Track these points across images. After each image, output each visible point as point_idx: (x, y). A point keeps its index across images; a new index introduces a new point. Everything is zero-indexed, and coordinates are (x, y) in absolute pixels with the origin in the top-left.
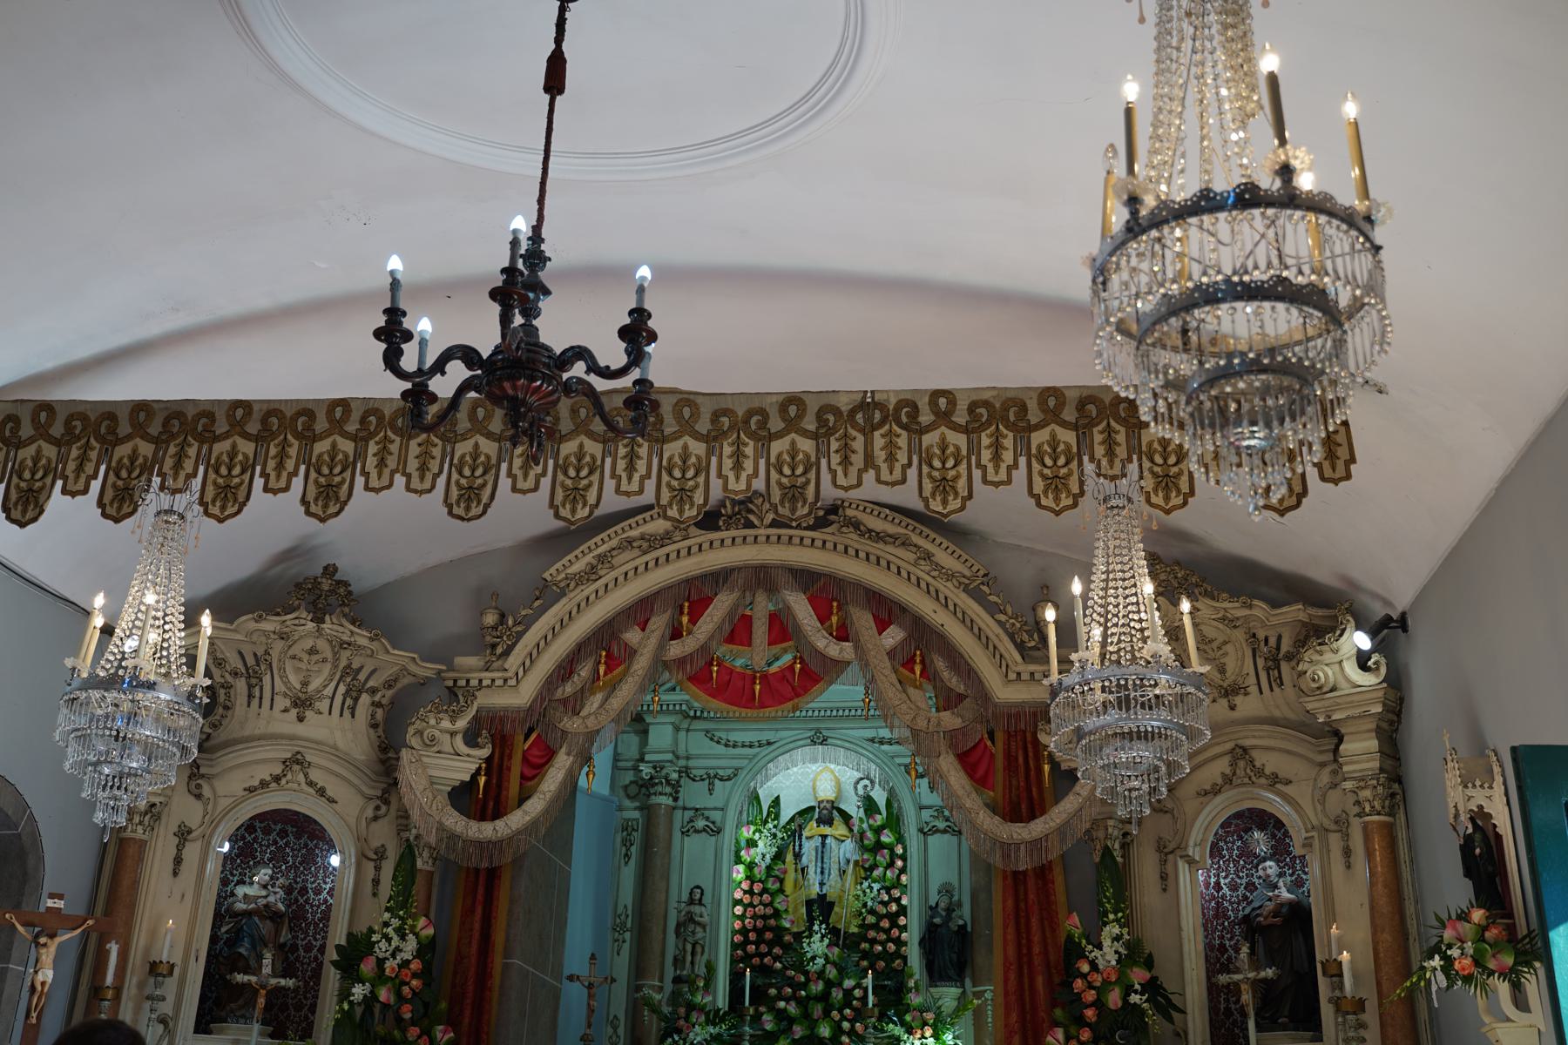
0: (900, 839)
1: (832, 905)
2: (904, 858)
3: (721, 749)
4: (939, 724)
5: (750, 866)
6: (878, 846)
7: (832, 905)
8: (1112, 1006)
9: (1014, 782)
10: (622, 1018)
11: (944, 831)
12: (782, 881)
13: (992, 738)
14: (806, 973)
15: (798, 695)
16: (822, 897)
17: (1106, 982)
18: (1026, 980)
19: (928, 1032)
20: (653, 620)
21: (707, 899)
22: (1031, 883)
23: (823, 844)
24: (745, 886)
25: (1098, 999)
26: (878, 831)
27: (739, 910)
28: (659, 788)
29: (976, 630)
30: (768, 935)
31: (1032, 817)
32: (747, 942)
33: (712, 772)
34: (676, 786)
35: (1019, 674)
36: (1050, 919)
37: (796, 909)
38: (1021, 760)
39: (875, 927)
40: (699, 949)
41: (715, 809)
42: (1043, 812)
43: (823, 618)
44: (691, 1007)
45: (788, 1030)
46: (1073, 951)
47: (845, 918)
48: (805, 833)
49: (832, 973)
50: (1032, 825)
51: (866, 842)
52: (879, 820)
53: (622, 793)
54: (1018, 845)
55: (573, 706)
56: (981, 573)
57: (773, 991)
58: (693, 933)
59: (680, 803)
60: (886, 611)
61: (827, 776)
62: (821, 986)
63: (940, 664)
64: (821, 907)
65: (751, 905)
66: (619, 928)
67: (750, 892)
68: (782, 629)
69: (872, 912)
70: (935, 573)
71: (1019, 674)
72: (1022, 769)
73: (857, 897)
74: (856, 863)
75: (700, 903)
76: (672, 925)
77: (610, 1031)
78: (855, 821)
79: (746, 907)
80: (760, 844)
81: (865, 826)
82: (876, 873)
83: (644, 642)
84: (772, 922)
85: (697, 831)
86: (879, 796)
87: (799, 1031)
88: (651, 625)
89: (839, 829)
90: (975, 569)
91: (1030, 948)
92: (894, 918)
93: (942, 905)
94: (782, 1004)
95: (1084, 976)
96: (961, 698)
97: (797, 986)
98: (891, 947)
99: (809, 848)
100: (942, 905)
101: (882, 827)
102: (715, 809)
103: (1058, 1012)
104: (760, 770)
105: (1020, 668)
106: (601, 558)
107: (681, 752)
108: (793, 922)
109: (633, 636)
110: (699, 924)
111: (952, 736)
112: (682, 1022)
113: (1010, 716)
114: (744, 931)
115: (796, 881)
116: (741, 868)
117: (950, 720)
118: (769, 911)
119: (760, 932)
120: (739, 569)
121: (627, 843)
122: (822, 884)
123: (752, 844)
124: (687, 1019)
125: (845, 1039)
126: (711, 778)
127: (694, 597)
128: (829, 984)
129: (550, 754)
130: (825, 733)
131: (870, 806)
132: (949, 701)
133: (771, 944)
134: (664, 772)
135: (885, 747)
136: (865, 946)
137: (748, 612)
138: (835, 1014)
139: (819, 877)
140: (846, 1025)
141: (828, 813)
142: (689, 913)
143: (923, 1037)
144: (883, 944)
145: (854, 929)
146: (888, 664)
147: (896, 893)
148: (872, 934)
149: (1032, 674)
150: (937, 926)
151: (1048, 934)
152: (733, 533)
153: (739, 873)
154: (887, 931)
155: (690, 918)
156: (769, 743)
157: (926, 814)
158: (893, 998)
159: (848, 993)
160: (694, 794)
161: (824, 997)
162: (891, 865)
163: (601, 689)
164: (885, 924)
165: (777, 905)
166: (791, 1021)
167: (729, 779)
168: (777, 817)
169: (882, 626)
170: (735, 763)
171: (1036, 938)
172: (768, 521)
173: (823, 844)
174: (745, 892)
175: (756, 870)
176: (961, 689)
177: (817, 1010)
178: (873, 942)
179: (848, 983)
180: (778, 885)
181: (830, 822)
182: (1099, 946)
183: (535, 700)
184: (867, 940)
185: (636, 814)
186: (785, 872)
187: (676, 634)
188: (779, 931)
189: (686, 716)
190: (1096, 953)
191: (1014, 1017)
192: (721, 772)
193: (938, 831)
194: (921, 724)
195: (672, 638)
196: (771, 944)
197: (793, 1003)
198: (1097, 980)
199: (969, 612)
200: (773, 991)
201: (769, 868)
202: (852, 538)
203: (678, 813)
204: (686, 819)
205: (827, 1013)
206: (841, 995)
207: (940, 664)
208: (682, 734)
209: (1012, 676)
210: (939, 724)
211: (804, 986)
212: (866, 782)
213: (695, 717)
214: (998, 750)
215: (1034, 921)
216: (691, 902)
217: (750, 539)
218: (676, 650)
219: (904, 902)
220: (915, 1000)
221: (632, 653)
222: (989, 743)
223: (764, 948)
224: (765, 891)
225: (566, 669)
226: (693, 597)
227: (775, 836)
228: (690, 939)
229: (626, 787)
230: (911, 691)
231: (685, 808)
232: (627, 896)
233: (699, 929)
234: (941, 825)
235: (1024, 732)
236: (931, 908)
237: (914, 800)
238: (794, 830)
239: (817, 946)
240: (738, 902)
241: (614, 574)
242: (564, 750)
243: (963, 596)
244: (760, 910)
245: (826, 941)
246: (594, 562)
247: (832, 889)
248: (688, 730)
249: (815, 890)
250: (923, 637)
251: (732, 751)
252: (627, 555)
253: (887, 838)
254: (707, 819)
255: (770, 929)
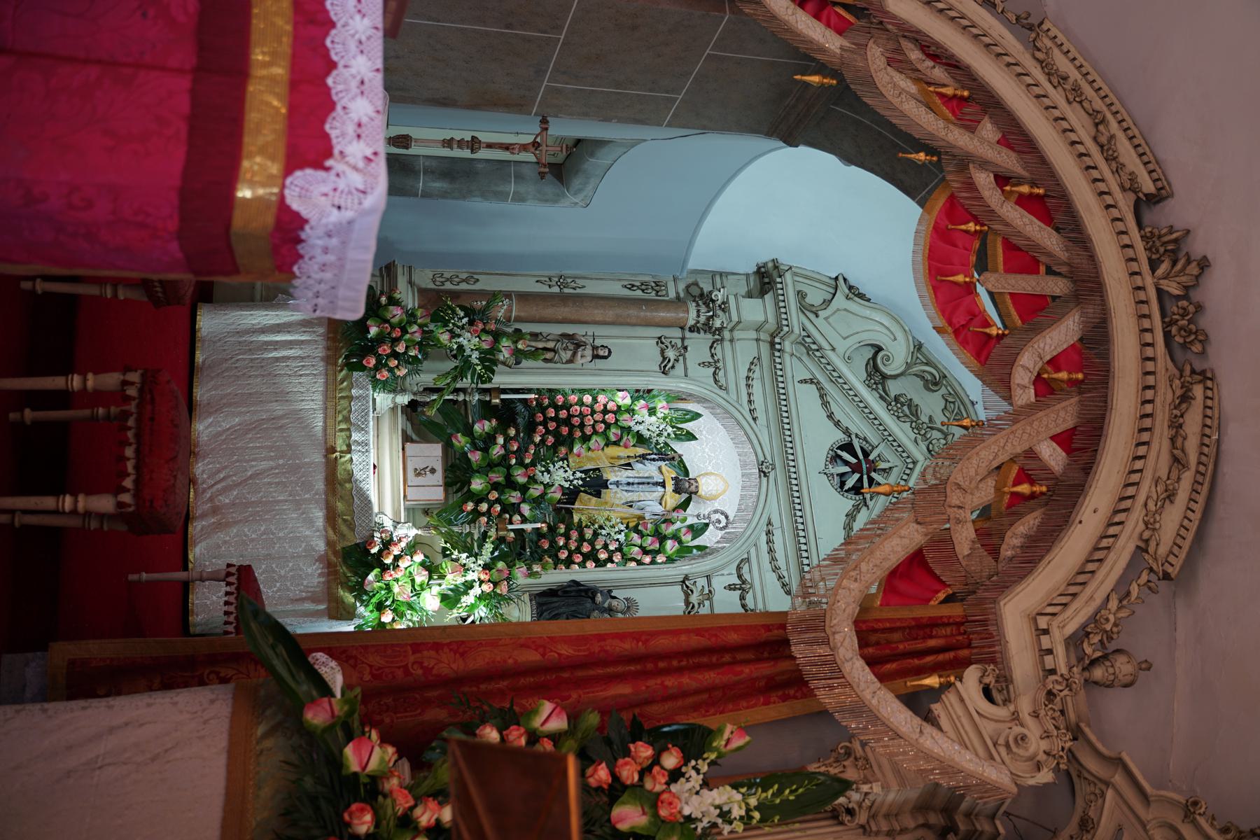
0: (670, 560)
1: (598, 495)
2: (653, 562)
3: (743, 373)
4: (958, 521)
5: (630, 411)
6: (662, 538)
7: (598, 495)
8: (617, 811)
9: (896, 636)
10: (477, 287)
11: (687, 603)
12: (616, 443)
13: (949, 599)
14: (533, 464)
15: (957, 333)
16: (605, 485)
17: (654, 801)
18: (620, 669)
19: (487, 588)
20: (1013, 155)
21: (600, 363)
22: (765, 669)
23: (657, 484)
24: (611, 406)
25: (625, 787)
26: (676, 537)
27: (588, 399)
28: (703, 309)
29: (1090, 567)
30: (565, 430)
31: (871, 662)
32: (557, 408)
33: (720, 364)
34: (707, 327)
35: (1046, 632)
36: (725, 698)
37: (590, 459)
38: (932, 643)
39: (582, 539)
40: (549, 355)
41: (686, 369)
42: (882, 678)
43: (1055, 363)
44: (497, 336)
45: (475, 447)
46: (694, 743)
47: (585, 508)
48: (662, 464)
49: (535, 491)
50: (860, 663)
51: (663, 526)
52: (687, 538)
53: (690, 281)
54: (826, 642)
55: (897, 61)
56: (1170, 570)
57: (512, 432)
58: (565, 349)
59: (688, 334)
60: (1083, 443)
61: (721, 486)
62: (522, 480)
63: (1028, 524)
64: (596, 484)
65: (593, 412)
66: (562, 281)
67: (605, 411)
68: (1034, 311)
69: (596, 534)
70: (1151, 506)
71: (1046, 632)
72: (920, 646)
73: (608, 519)
74: (641, 518)
75: (596, 357)
76: (569, 329)
77: (464, 276)
78: (681, 514)
79: (592, 407)
80: (653, 418)
81: (678, 524)
82: (635, 536)
83: (982, 141)
84: (578, 434)
85: (662, 352)
86: (710, 538)
87: (476, 457)
88: (1005, 150)
89: (672, 500)
90: (1172, 559)
91: (667, 672)
92: (592, 556)
93: (615, 603)
94: (501, 440)
95: (656, 761)
96: (994, 552)
97: (520, 454)
98: (563, 555)
99: (650, 470)
100: (615, 603)
101: (680, 542)
102: (686, 369)
103: (593, 719)
104: (725, 415)
105: (1056, 632)
106: (1076, 89)
107: (737, 334)
108: (579, 455)
109: (988, 130)
110: (574, 354)
111: (943, 542)
112: (481, 326)
113: (984, 623)
114: (567, 406)
115: (619, 458)
116: (628, 401)
117: (964, 538)
118: (588, 430)
119: (567, 421)
120: (1092, 258)
121: (644, 287)
122: (617, 484)
123: (652, 412)
124: (484, 330)
125: (470, 506)
126: (714, 364)
127: (1050, 202)
128: (524, 489)
129: (840, 32)
130: (772, 475)
131: (697, 531)
132: (989, 538)
133: (556, 434)
134: (719, 312)
135: (764, 538)
136: (562, 529)
137: (1042, 269)
138: (494, 495)
139: (624, 481)
140: (484, 507)
141: (686, 488)
142: (585, 344)
143: (481, 582)
144: (566, 546)
145: (576, 518)
146: (1019, 450)
147: (617, 557)
148: (574, 535)
149: (1050, 652)
150: (593, 599)
151: (690, 700)
152: (1140, 245)
153: (623, 399)
154: (578, 550)
155: (579, 345)
156: (755, 419)
157: (702, 582)
158: (518, 550)
159: (515, 509)
160: (699, 346)
161: (510, 484)
162: (645, 552)
163: (921, 91)
164: (586, 548)
165: (594, 438)
166: (486, 450)
167: (716, 381)
168: (678, 438)
169: (1064, 440)
170: (732, 387)
171: (687, 681)
172: (1165, 285)
173: (657, 484)
174: (605, 406)
175: (626, 416)
176: (1006, 552)
177: (498, 476)
178: (567, 536)
179: (526, 509)
180: (613, 438)
181: (677, 490)
182: (707, 784)
183: (894, 17)
184: (568, 529)
185: (672, 294)
186: (626, 447)
187: (1002, 180)
188: (569, 442)
189: (773, 336)
190: (696, 780)
191: (566, 650)
192: (721, 373)
193: (687, 596)
194: (955, 498)
195: (997, 177)
196: (556, 434)
197: (502, 452)
198: (655, 784)
199: (1112, 556)
200: (512, 432)
201: (629, 429)
202: (1165, 396)
203: (677, 333)
204: (674, 341)
205: (495, 486)
206: (513, 500)
207: (1028, 524)
208: (754, 335)
209: (1043, 622)
210: (958, 521)
211: (520, 463)
212: (723, 524)
213: (772, 344)
214: (935, 608)
215: (710, 677)
216: (595, 348)
217: (1134, 266)
218: (984, 180)
219: (609, 565)
220: (520, 575)
221: (971, 127)
222: (941, 596)
223: (552, 426)
224: (608, 426)
225: (936, 53)
226: (1050, 204)
227: (659, 435)
228: (559, 345)
229: (696, 284)
230: (991, 482)
231: (683, 339)
232: (592, 288)
233: (569, 353)
234: (694, 599)
235: (969, 646)
236: (610, 591)
237: (716, 569)
238: (665, 455)
239: (560, 476)
240: (595, 400)
241: (1062, 102)
242: (846, 44)
243: (1131, 547)
244: (589, 421)
245: (567, 485)
246: (1071, 80)
247: (616, 496)
248: (757, 340)
249: (611, 477)
250: (1063, 498)
251: (743, 383)
252: (1088, 121)
253: (670, 545)
254: (677, 360)
255: (571, 433)
